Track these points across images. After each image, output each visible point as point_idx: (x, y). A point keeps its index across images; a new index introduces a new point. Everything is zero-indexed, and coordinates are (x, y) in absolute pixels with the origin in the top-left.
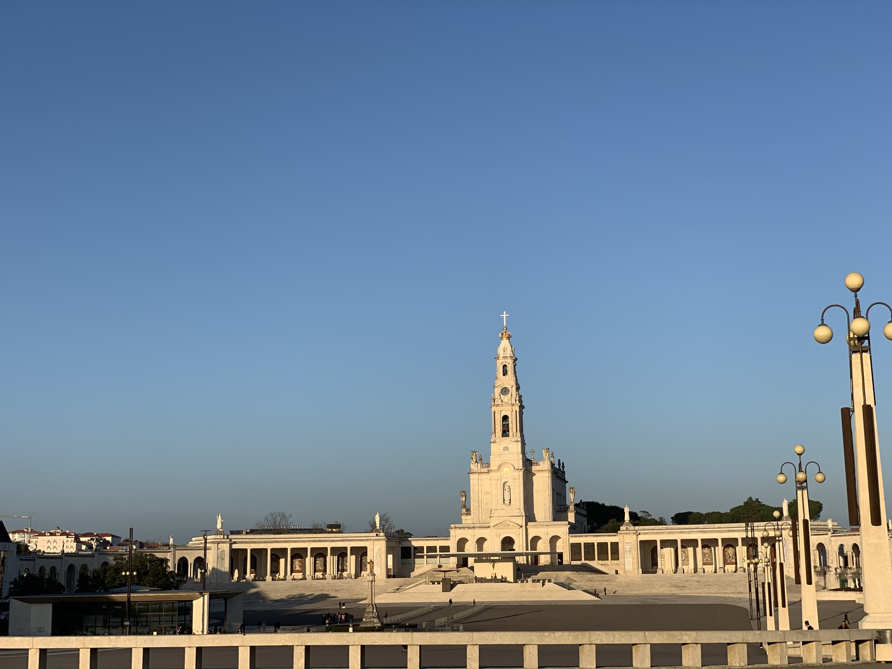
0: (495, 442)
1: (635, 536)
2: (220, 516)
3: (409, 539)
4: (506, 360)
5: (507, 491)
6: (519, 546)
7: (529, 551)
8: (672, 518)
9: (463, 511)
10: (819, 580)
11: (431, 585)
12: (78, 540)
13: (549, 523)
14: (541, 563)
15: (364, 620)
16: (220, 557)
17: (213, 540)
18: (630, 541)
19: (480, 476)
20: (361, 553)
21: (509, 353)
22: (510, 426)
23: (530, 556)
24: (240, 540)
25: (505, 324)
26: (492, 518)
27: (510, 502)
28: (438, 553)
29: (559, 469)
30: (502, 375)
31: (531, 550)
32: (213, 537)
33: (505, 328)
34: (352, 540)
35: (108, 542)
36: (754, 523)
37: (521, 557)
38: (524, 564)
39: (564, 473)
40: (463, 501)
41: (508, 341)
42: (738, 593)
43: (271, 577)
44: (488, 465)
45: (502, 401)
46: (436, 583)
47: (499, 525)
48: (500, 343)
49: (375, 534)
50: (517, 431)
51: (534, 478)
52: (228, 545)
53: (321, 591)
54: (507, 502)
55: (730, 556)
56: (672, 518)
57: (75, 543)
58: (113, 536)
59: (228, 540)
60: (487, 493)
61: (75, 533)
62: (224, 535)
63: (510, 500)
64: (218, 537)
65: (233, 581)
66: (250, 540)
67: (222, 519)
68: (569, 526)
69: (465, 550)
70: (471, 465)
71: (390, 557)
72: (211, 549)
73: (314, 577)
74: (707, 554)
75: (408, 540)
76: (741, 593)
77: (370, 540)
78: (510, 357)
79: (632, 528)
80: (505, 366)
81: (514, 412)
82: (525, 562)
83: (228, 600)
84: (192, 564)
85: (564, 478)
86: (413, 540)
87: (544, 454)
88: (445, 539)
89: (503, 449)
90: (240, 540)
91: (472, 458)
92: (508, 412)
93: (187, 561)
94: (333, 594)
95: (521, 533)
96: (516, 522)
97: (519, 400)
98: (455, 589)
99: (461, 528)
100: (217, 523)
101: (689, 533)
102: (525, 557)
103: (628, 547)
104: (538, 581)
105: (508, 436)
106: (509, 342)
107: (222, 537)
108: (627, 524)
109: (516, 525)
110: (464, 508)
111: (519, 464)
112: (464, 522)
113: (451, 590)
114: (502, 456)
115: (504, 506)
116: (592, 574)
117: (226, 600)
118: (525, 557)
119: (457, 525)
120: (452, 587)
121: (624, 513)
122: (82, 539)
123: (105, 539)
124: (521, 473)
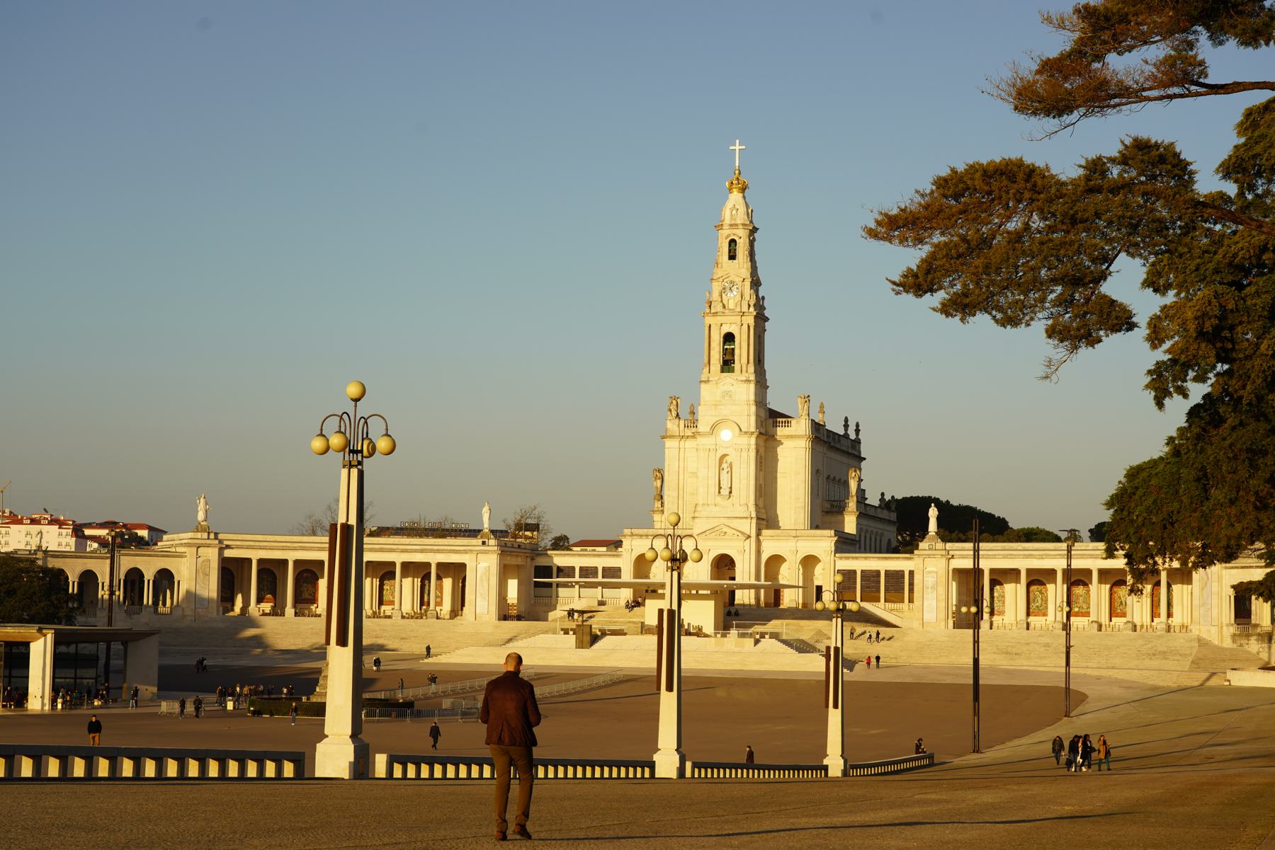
0: (708, 381)
1: (944, 561)
2: (202, 500)
3: (549, 552)
4: (735, 231)
5: (726, 471)
6: (744, 572)
7: (763, 582)
8: (1090, 531)
9: (656, 506)
10: (1261, 650)
11: (561, 636)
12: (80, 534)
13: (799, 533)
14: (785, 604)
15: (318, 690)
16: (200, 572)
17: (190, 541)
18: (934, 569)
19: (682, 443)
20: (457, 571)
21: (741, 218)
22: (737, 352)
23: (762, 591)
24: (238, 543)
25: (737, 165)
26: (696, 520)
27: (731, 492)
28: (577, 578)
29: (846, 436)
30: (727, 257)
31: (765, 581)
32: (190, 535)
33: (737, 172)
34: (438, 551)
35: (142, 538)
36: (981, 544)
37: (746, 591)
38: (750, 605)
39: (857, 442)
40: (657, 488)
41: (741, 195)
42: (1108, 668)
43: (293, 610)
44: (693, 422)
45: (724, 307)
46: (571, 633)
47: (707, 533)
48: (727, 198)
49: (480, 541)
50: (748, 363)
51: (780, 450)
52: (216, 550)
53: (376, 637)
54: (725, 491)
55: (1121, 602)
56: (1090, 531)
57: (74, 539)
58: (151, 529)
59: (217, 542)
60: (695, 474)
61: (74, 522)
62: (209, 533)
63: (731, 488)
64: (199, 535)
65: (231, 614)
66: (257, 544)
67: (206, 504)
68: (836, 538)
69: (651, 575)
70: (668, 422)
71: (513, 586)
72: (186, 556)
73: (380, 613)
74: (1081, 596)
75: (547, 554)
76: (1113, 668)
77: (471, 551)
78: (743, 225)
79: (940, 545)
80: (733, 242)
81: (745, 327)
82: (753, 602)
83: (131, 645)
84: (76, 584)
85: (857, 453)
86: (555, 554)
87: (800, 406)
88: (614, 555)
90: (238, 543)
91: (670, 410)
92: (734, 326)
93: (143, 576)
94: (391, 645)
95: (747, 548)
96: (739, 529)
97: (754, 305)
98: (599, 645)
99: (641, 536)
100: (197, 512)
101: (1041, 557)
102: (753, 590)
103: (930, 580)
104: (751, 635)
105: (732, 370)
106: (744, 197)
107: (205, 535)
108: (932, 539)
109: (739, 534)
110: (658, 500)
111: (750, 423)
112: (657, 525)
113: (591, 645)
115: (719, 499)
116: (866, 626)
117: (125, 644)
118: (753, 591)
119: (636, 531)
120: (595, 639)
121: (928, 519)
122: (88, 532)
123: (137, 533)
124: (753, 440)
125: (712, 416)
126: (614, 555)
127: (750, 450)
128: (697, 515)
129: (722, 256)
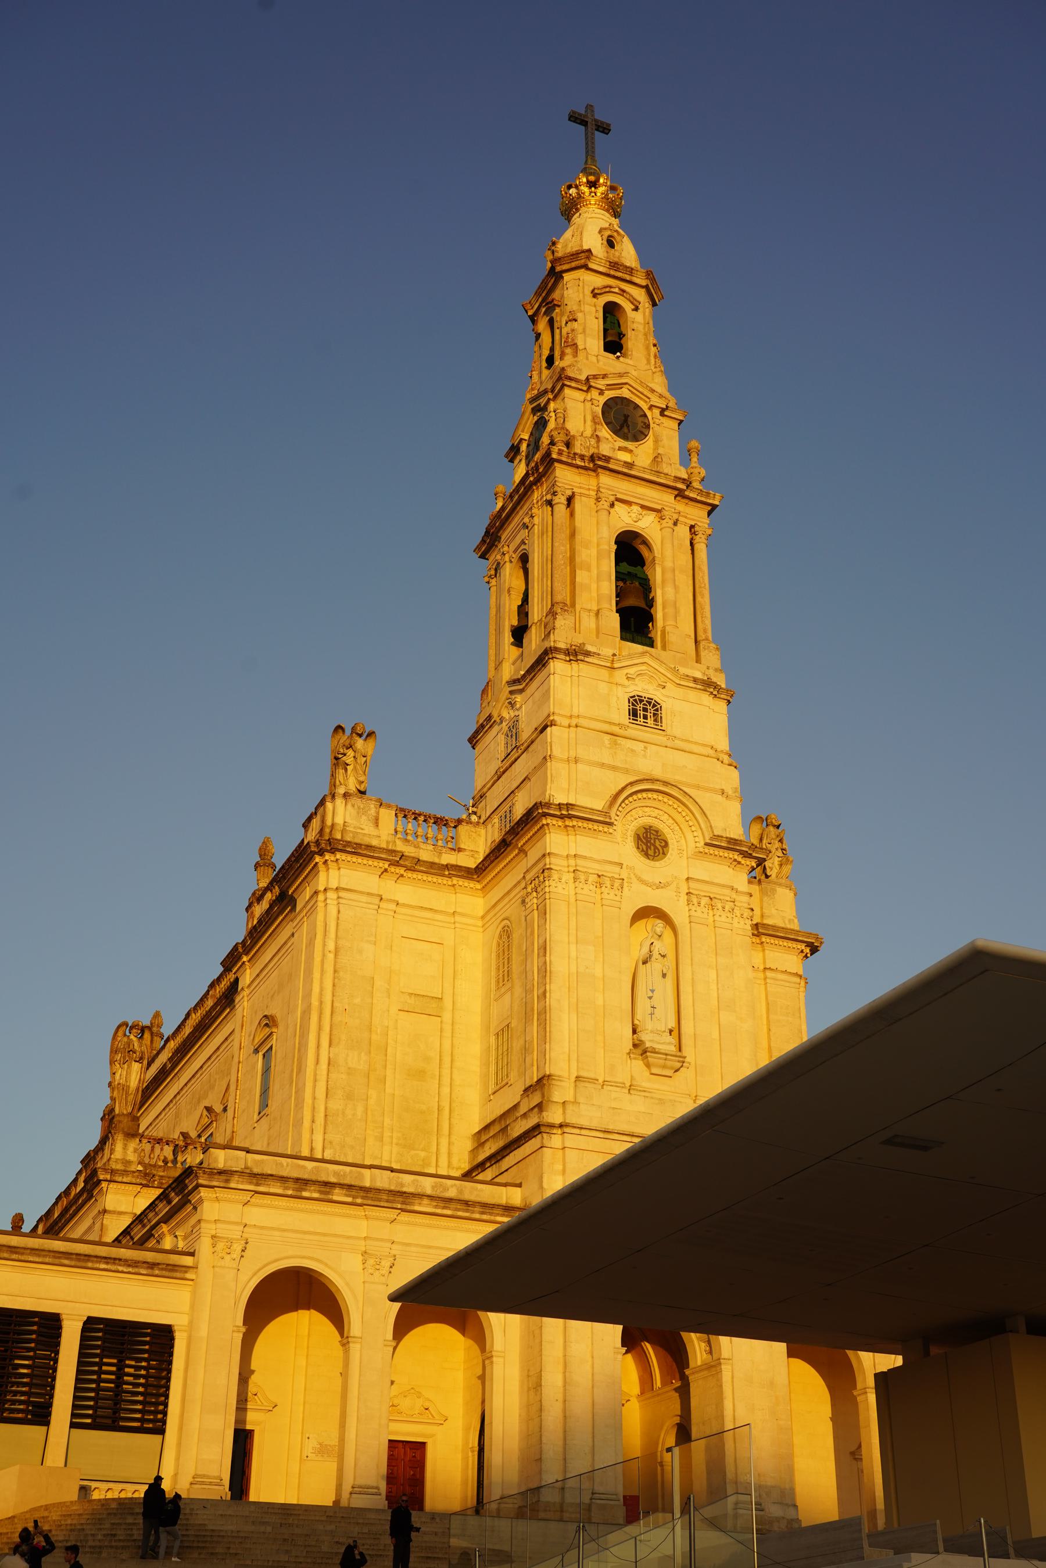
81: (683, 531)
89: (625, 707)
114: (620, 740)
125: (603, 765)
126: (152, 1265)
127: (737, 912)
128: (554, 1115)
129: (584, 331)
